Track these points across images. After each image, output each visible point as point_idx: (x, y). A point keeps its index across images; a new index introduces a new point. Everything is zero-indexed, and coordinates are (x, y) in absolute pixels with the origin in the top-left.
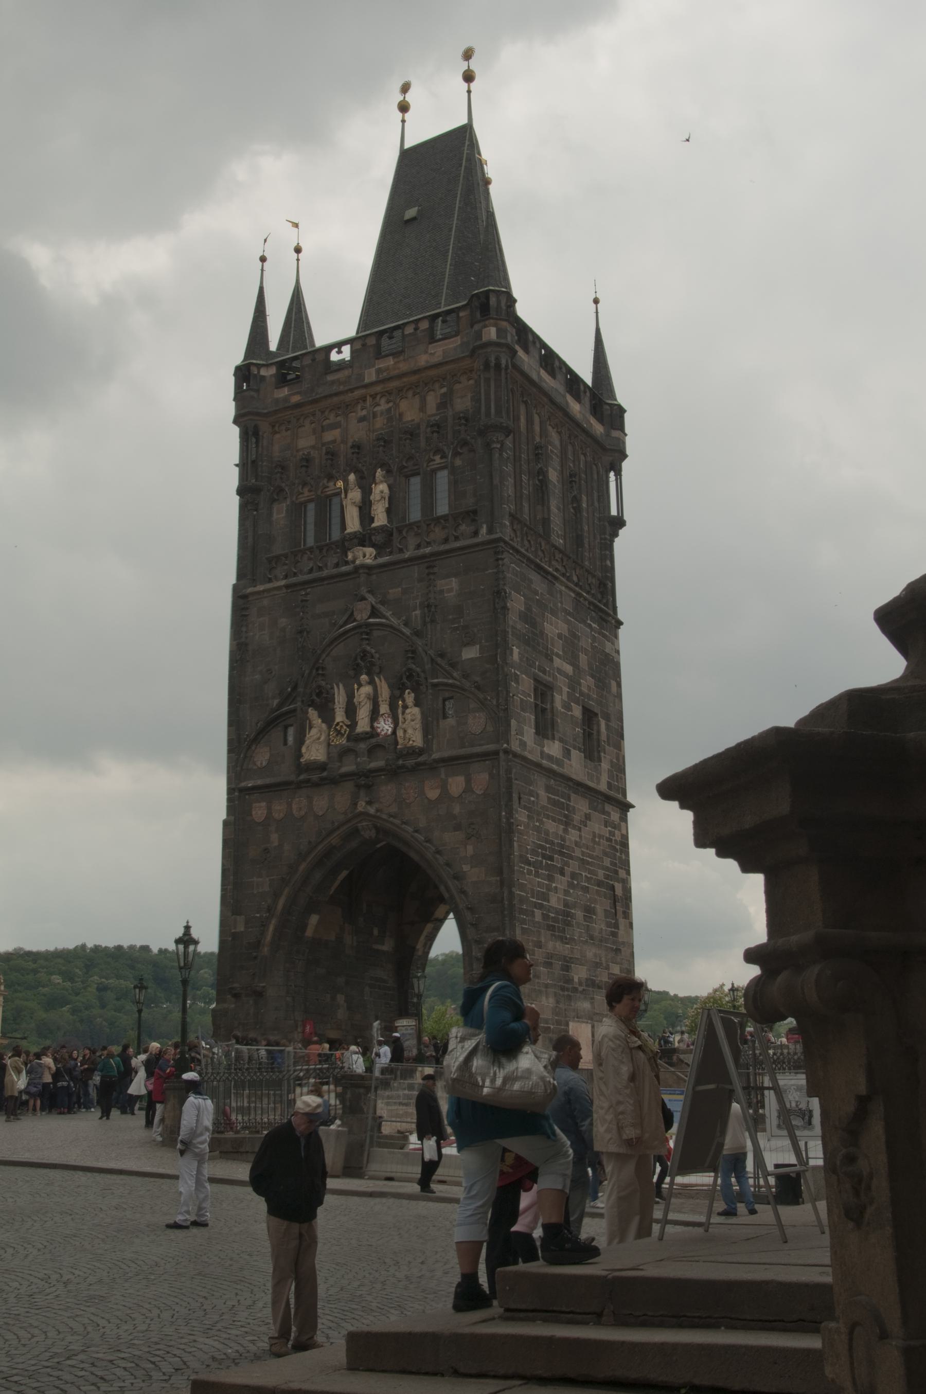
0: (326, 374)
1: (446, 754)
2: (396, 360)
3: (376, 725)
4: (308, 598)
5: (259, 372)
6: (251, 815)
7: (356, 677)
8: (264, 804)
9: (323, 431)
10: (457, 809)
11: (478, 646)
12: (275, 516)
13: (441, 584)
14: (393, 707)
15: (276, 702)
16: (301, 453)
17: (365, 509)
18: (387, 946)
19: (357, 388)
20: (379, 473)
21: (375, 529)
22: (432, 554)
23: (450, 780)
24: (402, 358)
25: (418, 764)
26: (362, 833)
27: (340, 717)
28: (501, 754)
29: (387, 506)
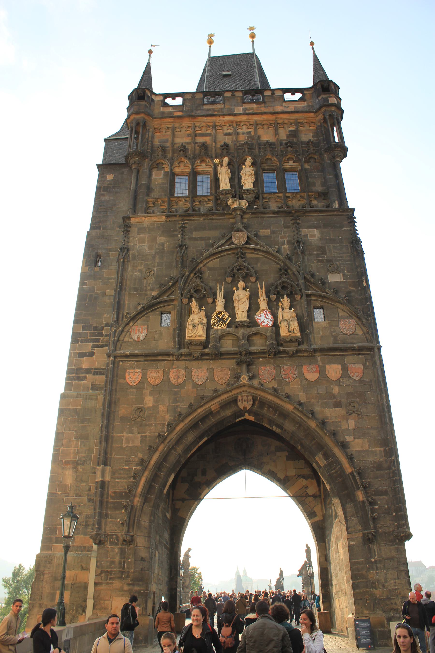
0: (204, 104)
1: (325, 345)
2: (258, 106)
4: (185, 225)
5: (151, 95)
6: (125, 379)
7: (235, 282)
8: (139, 370)
9: (196, 135)
10: (336, 390)
11: (342, 274)
12: (154, 177)
13: (304, 231)
14: (269, 307)
15: (155, 293)
16: (178, 145)
18: (169, 515)
19: (229, 115)
21: (248, 190)
22: (297, 211)
23: (327, 367)
24: (263, 105)
26: (239, 403)
28: (376, 350)
29: (254, 180)
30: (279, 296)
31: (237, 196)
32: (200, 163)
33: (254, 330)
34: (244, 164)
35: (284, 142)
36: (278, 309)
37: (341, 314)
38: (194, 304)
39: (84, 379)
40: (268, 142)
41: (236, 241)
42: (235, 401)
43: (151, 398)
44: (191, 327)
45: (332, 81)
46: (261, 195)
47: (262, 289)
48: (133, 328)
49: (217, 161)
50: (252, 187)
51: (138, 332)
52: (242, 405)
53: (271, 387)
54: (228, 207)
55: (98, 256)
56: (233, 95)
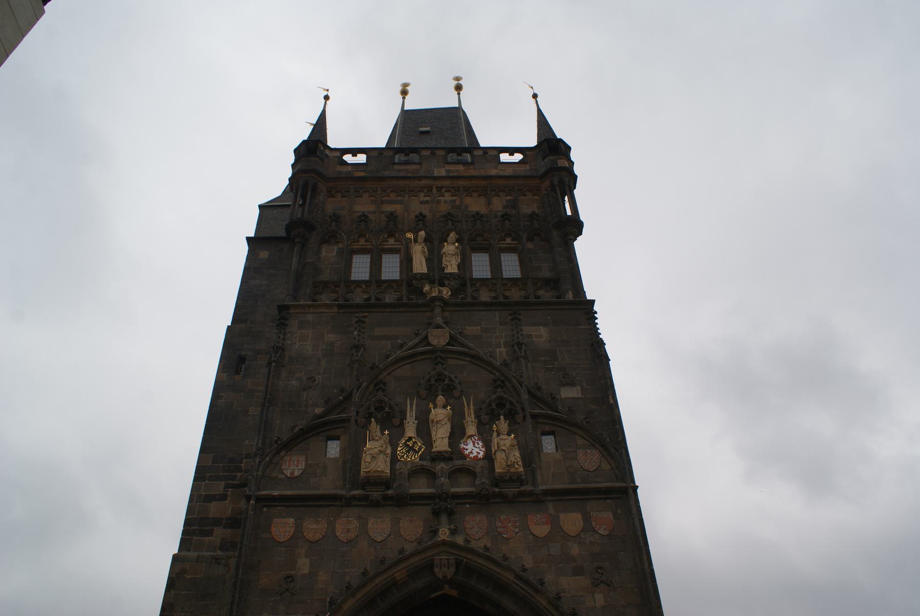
0: (394, 164)
3: (462, 446)
4: (365, 319)
6: (270, 532)
9: (382, 202)
10: (575, 550)
11: (579, 388)
13: (526, 330)
14: (480, 433)
15: (318, 411)
17: (434, 258)
19: (427, 177)
20: (453, 235)
21: (451, 274)
23: (562, 516)
24: (471, 167)
25: (521, 494)
26: (436, 570)
27: (410, 430)
28: (631, 491)
30: (494, 417)
31: (437, 281)
32: (388, 236)
33: (458, 463)
34: (446, 241)
35: (500, 214)
36: (491, 435)
37: (580, 441)
38: (374, 426)
39: (210, 533)
40: (478, 213)
41: (434, 341)
42: (429, 566)
43: (307, 561)
44: (368, 459)
45: (561, 140)
46: (468, 281)
47: (469, 408)
48: (287, 458)
49: (410, 235)
50: (456, 271)
51: (294, 465)
52: (439, 573)
53: (483, 545)
54: (423, 295)
55: (242, 359)
56: (433, 154)
